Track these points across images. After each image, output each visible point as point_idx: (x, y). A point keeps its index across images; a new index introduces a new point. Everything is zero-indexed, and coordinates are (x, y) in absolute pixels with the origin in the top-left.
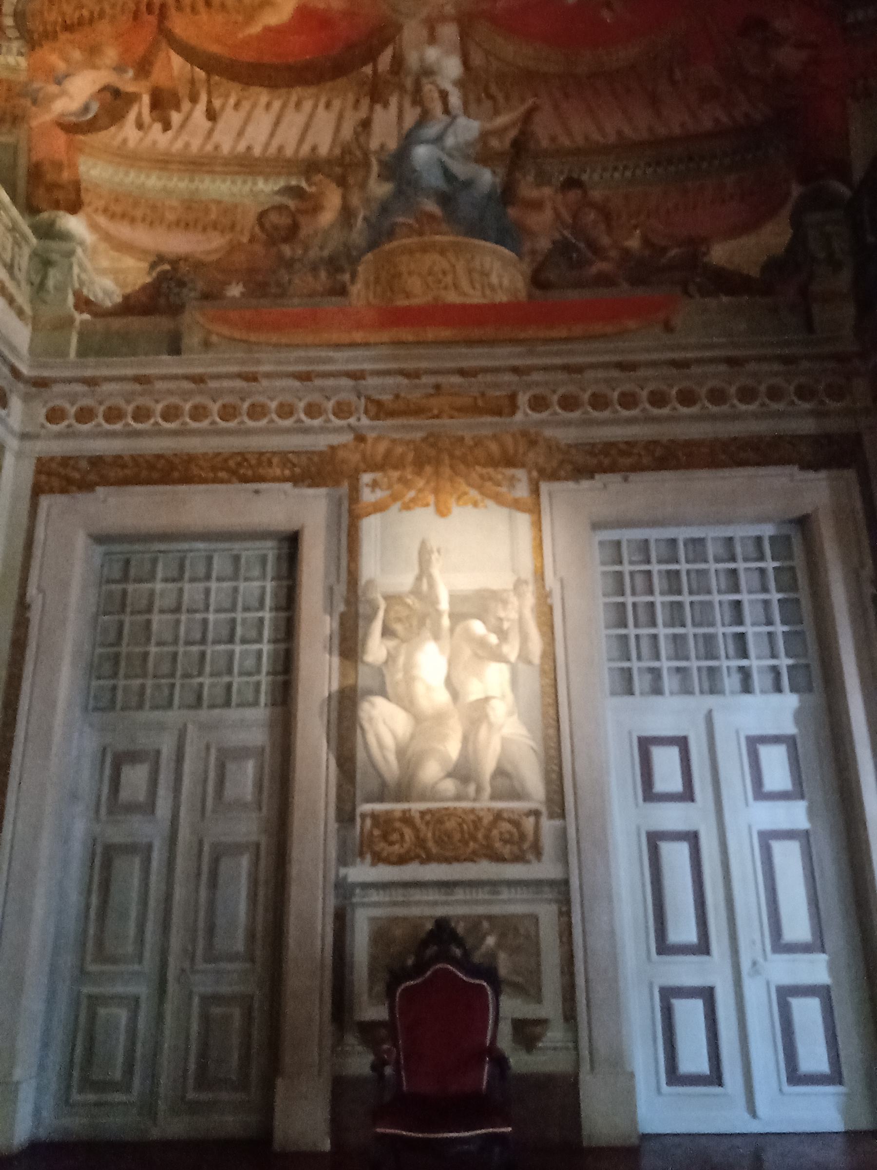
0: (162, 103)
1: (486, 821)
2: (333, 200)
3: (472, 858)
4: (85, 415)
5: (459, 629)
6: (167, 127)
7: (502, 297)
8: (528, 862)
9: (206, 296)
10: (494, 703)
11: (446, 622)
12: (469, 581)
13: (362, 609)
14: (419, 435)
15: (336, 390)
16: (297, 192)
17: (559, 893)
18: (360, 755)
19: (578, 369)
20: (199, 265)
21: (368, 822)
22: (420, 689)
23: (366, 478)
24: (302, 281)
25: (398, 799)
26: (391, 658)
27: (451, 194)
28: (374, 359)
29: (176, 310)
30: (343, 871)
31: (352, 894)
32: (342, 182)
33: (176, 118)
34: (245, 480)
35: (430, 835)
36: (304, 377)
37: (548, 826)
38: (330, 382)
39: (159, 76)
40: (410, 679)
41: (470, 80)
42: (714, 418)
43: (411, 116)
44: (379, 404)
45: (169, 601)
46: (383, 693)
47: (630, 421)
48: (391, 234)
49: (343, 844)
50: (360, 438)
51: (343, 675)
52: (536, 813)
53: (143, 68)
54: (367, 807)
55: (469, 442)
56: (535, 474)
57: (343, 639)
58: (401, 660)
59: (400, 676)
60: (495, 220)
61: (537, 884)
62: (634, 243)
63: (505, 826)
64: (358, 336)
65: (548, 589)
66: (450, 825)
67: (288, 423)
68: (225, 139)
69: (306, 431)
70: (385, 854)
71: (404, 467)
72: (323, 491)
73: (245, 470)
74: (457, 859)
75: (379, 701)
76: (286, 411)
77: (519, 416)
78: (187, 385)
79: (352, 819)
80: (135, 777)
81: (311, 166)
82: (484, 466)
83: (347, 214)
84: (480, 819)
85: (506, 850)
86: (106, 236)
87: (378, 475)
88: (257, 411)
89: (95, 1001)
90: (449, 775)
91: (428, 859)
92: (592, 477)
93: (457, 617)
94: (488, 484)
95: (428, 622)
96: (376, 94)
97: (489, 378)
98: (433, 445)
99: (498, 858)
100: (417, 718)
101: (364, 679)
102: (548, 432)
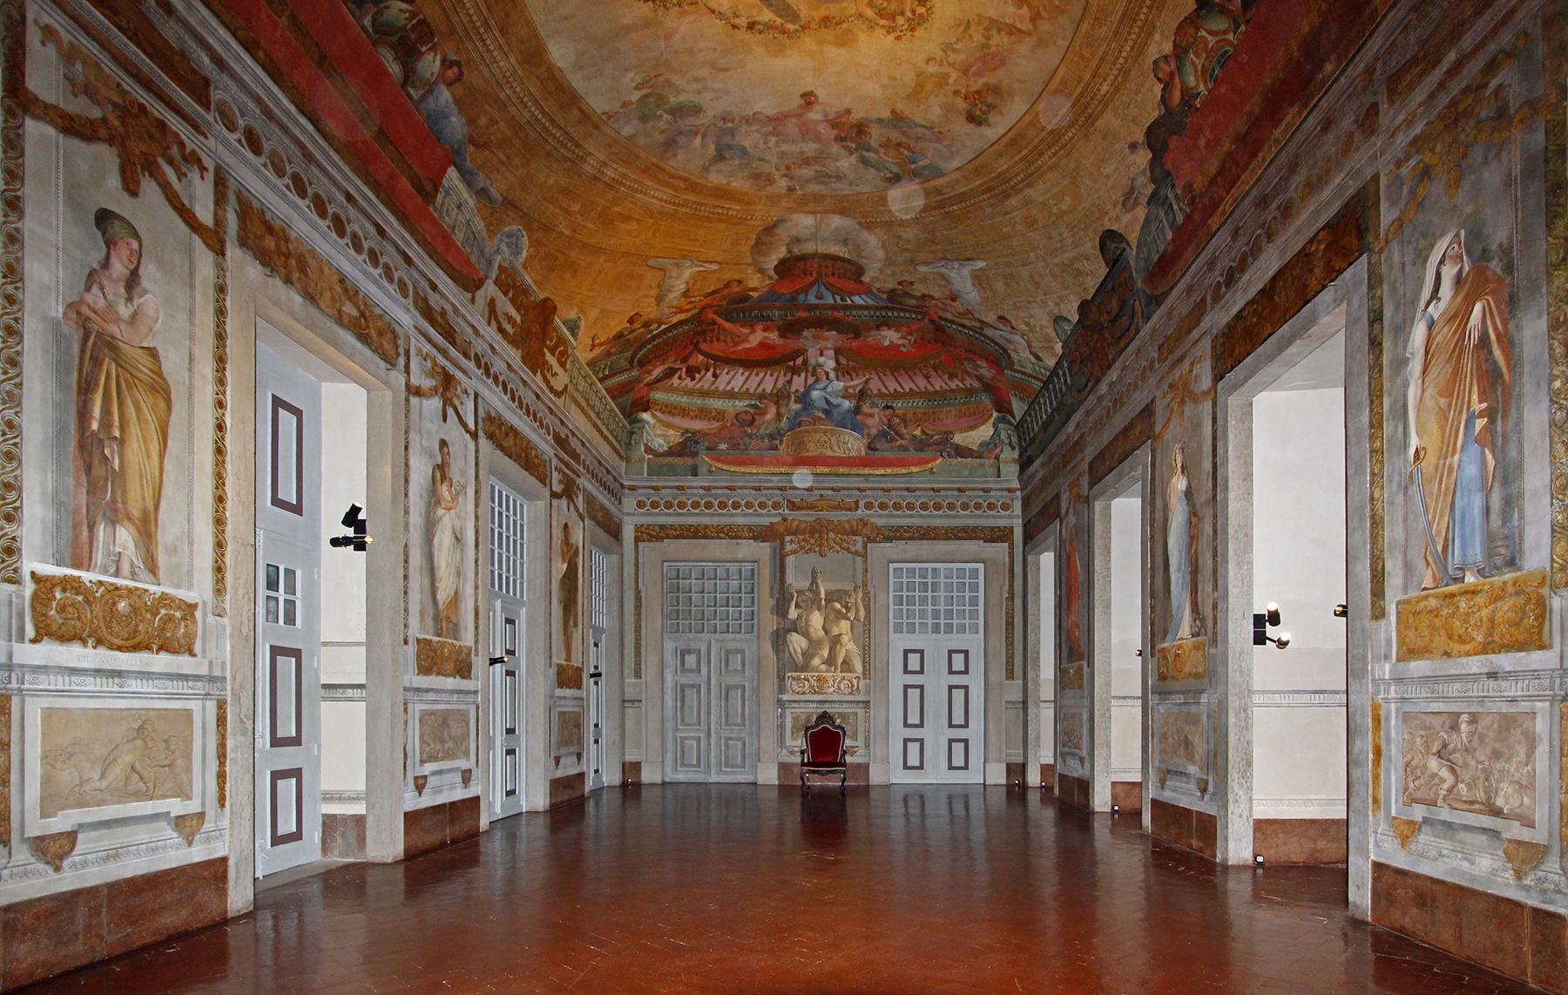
2: (773, 410)
9: (708, 449)
12: (832, 586)
19: (889, 490)
23: (788, 538)
26: (799, 617)
29: (695, 454)
32: (777, 403)
34: (732, 538)
36: (758, 489)
42: (948, 516)
43: (811, 380)
47: (911, 516)
48: (800, 424)
50: (785, 520)
62: (918, 432)
76: (749, 505)
81: (762, 397)
83: (779, 416)
88: (736, 505)
96: (795, 371)
102: (873, 520)
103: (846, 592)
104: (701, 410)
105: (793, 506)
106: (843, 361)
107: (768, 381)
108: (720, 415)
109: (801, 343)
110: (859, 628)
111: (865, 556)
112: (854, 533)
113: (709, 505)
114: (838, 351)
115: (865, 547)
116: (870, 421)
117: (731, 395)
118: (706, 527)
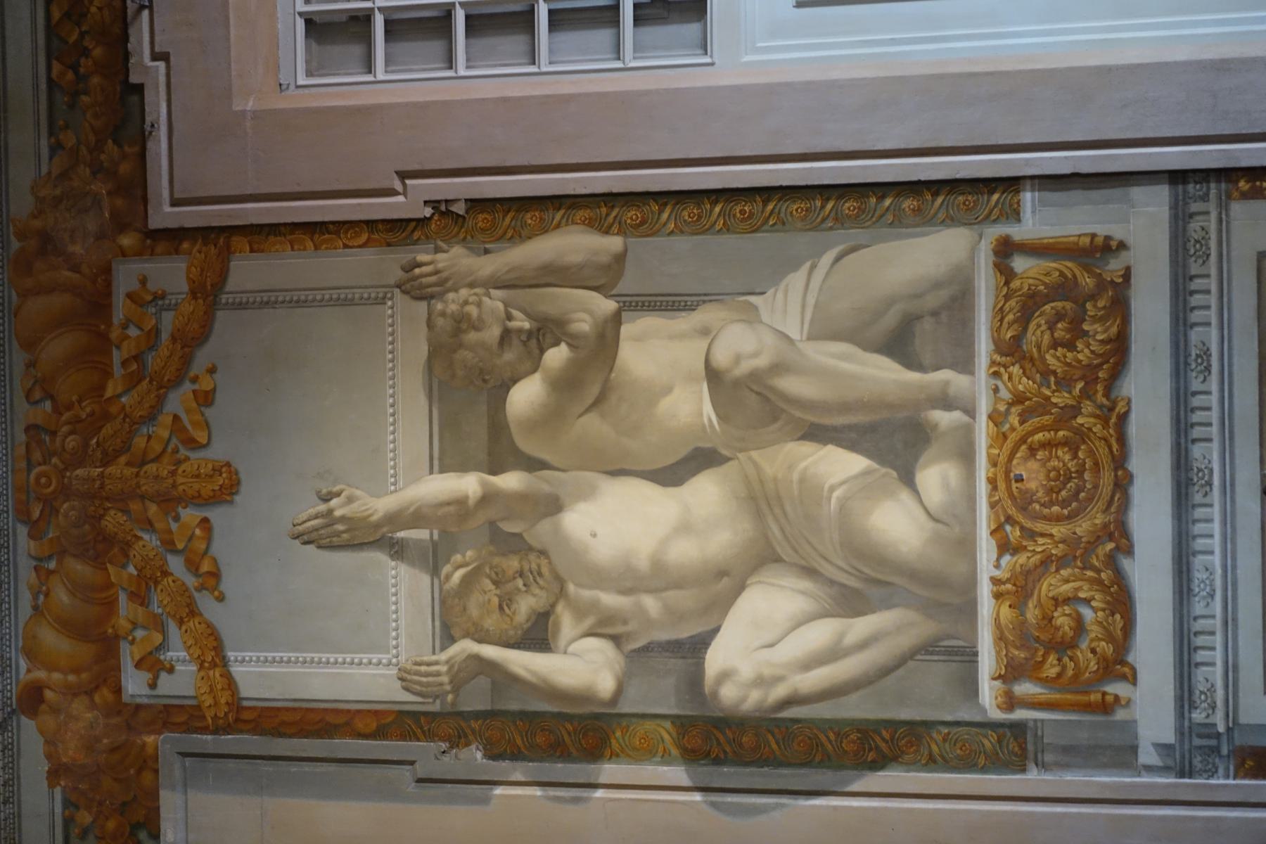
1: (1024, 385)
5: (527, 445)
8: (1127, 274)
10: (721, 358)
11: (511, 481)
13: (476, 699)
17: (1205, 198)
18: (855, 708)
21: (1025, 688)
22: (685, 552)
25: (969, 610)
26: (606, 627)
30: (1147, 756)
31: (1207, 730)
35: (1057, 531)
37: (1037, 219)
40: (660, 577)
46: (698, 645)
51: (646, 752)
52: (1005, 249)
54: (988, 692)
56: (126, 241)
57: (558, 750)
58: (610, 600)
61: (1182, 249)
63: (1037, 334)
65: (428, 212)
66: (1032, 474)
70: (1105, 648)
71: (109, 585)
72: (170, 801)
75: (716, 659)
79: (1018, 729)
82: (107, 374)
84: (1019, 399)
85: (1098, 332)
87: (128, 655)
90: (908, 480)
91: (1119, 535)
92: (139, 89)
93: (500, 451)
94: (153, 361)
95: (510, 527)
98: (50, 508)
99: (1119, 349)
101: (659, 697)
110: (670, 256)
111: (222, 238)
112: (97, 304)
115: (174, 237)
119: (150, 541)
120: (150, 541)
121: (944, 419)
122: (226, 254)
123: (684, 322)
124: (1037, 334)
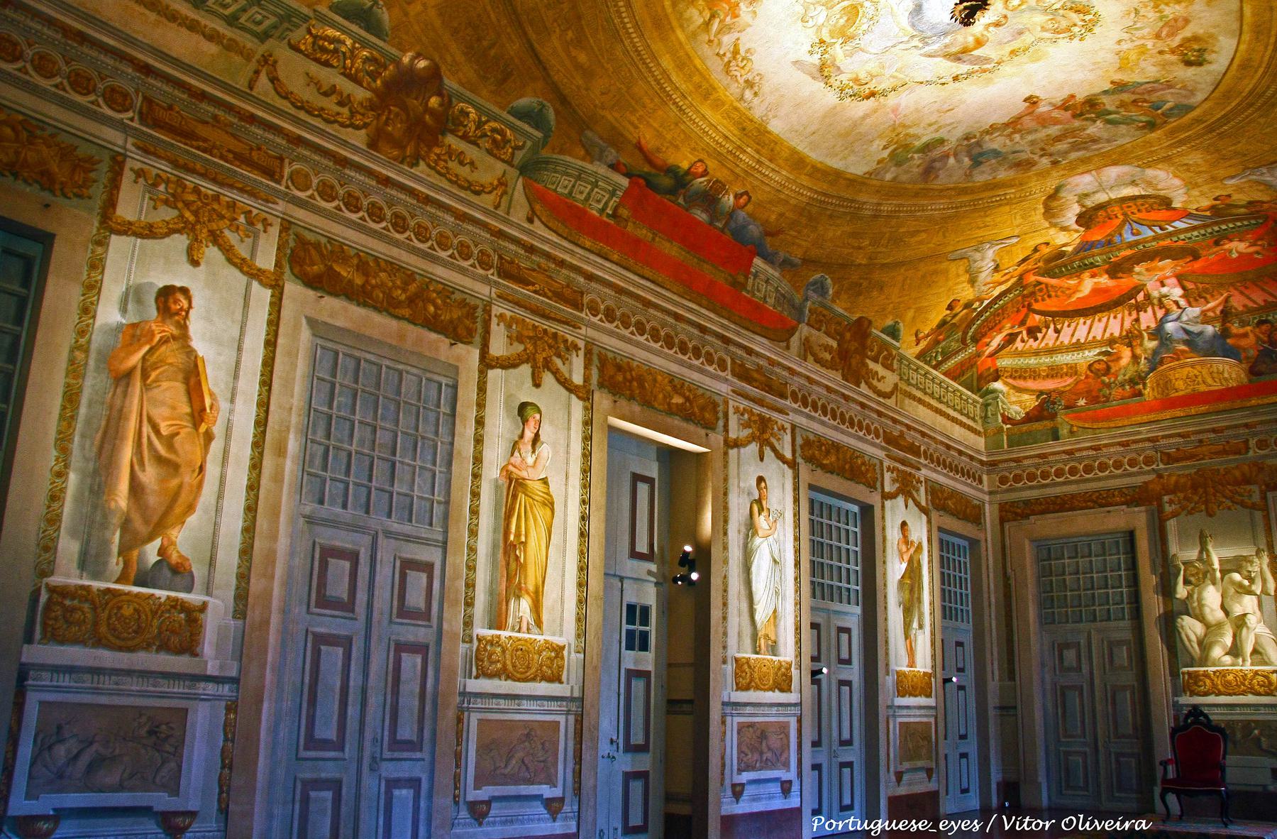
0: (1032, 332)
2: (1126, 354)
3: (1243, 693)
4: (1017, 478)
5: (1226, 577)
6: (1036, 339)
7: (1233, 384)
9: (1067, 407)
11: (1218, 575)
12: (1230, 552)
13: (1172, 570)
14: (1193, 471)
15: (1143, 450)
16: (1106, 353)
18: (1179, 645)
20: (1061, 393)
22: (1207, 611)
23: (1166, 498)
24: (1117, 392)
26: (1190, 595)
27: (1191, 340)
28: (1162, 429)
29: (1053, 416)
32: (1130, 345)
33: (1040, 335)
34: (1101, 506)
38: (1140, 445)
39: (1029, 323)
40: (1201, 606)
41: (1187, 295)
44: (1168, 455)
45: (1072, 569)
48: (1161, 363)
49: (1174, 686)
50: (1160, 476)
51: (1165, 604)
53: (1022, 323)
55: (1222, 472)
58: (1195, 596)
59: (1195, 604)
60: (1221, 346)
64: (1152, 417)
66: (1230, 677)
67: (1119, 472)
68: (1065, 338)
69: (1130, 475)
72: (1143, 508)
73: (1100, 500)
74: (1235, 694)
75: (1185, 617)
76: (1118, 465)
77: (1251, 453)
78: (1065, 457)
80: (1070, 655)
81: (1112, 342)
83: (1135, 358)
85: (1262, 690)
86: (1014, 387)
87: (1172, 497)
88: (1103, 467)
89: (1067, 754)
91: (1219, 694)
93: (1224, 572)
96: (1139, 308)
97: (1230, 432)
99: (1259, 694)
100: (1208, 626)
102: (1269, 462)
103: (1245, 559)
104: (1051, 368)
105: (1169, 459)
106: (1190, 286)
107: (1114, 325)
108: (1073, 370)
109: (1136, 279)
111: (1265, 509)
112: (1247, 481)
113: (1073, 471)
114: (1180, 279)
115: (1264, 498)
116: (1243, 342)
117: (1078, 346)
118: (1073, 496)
119: (1196, 498)
120: (1196, 498)
121: (1240, 660)
122: (1263, 510)
123: (1256, 608)
124: (1260, 678)
